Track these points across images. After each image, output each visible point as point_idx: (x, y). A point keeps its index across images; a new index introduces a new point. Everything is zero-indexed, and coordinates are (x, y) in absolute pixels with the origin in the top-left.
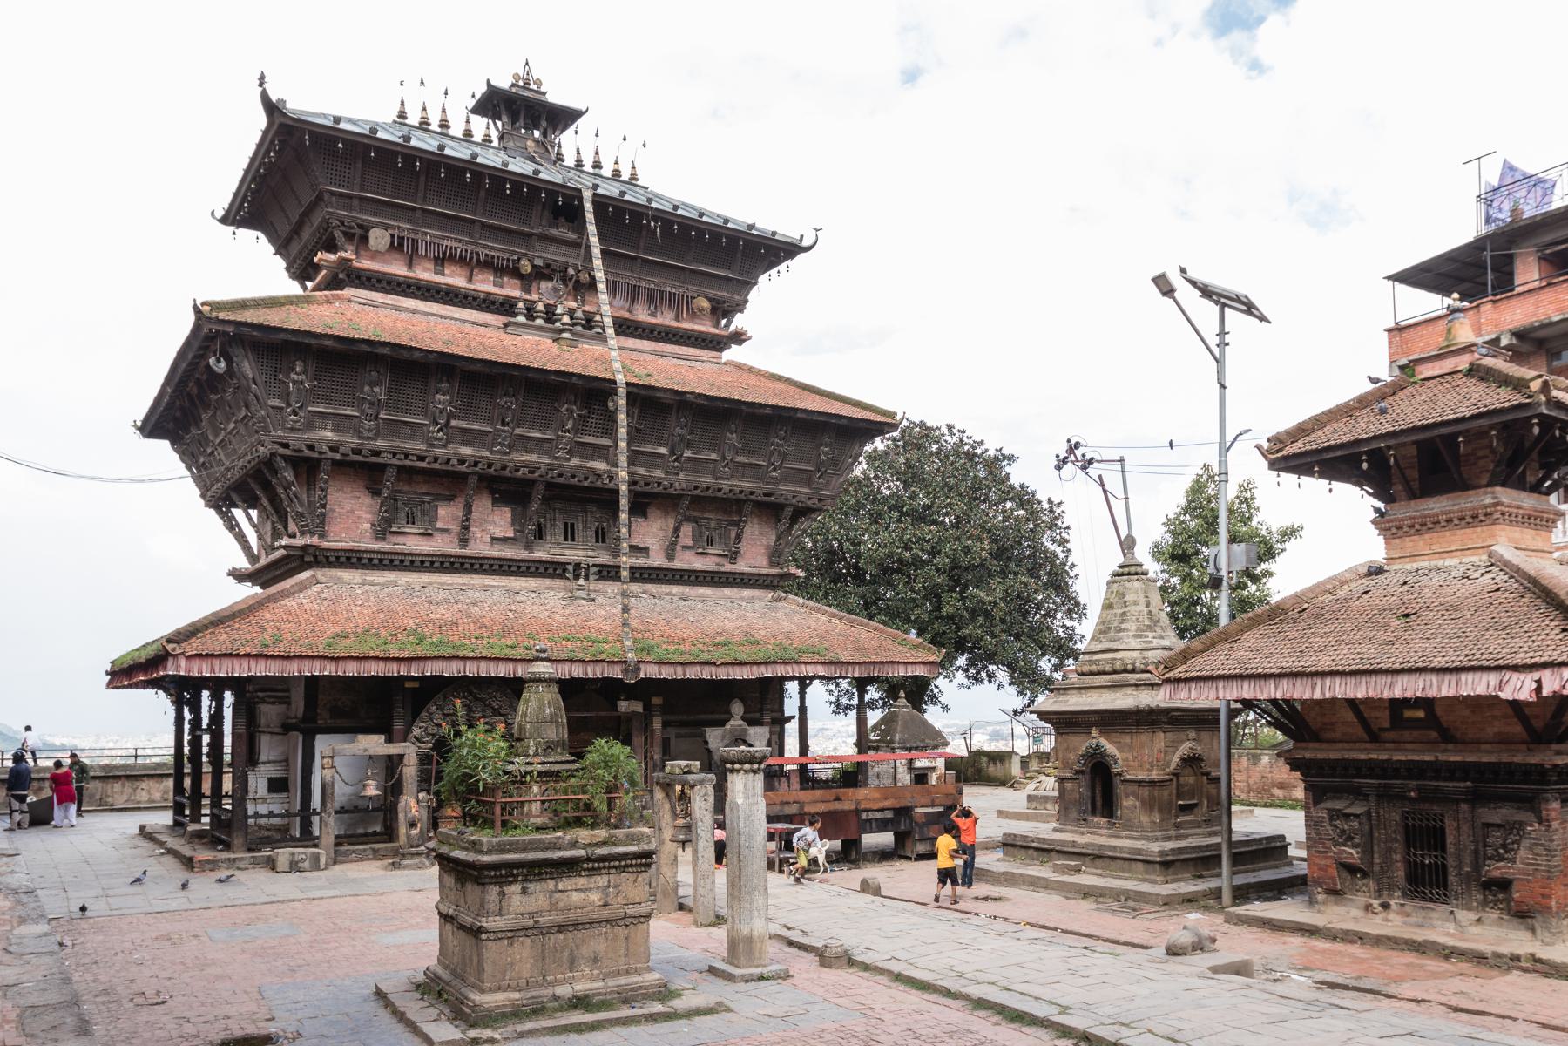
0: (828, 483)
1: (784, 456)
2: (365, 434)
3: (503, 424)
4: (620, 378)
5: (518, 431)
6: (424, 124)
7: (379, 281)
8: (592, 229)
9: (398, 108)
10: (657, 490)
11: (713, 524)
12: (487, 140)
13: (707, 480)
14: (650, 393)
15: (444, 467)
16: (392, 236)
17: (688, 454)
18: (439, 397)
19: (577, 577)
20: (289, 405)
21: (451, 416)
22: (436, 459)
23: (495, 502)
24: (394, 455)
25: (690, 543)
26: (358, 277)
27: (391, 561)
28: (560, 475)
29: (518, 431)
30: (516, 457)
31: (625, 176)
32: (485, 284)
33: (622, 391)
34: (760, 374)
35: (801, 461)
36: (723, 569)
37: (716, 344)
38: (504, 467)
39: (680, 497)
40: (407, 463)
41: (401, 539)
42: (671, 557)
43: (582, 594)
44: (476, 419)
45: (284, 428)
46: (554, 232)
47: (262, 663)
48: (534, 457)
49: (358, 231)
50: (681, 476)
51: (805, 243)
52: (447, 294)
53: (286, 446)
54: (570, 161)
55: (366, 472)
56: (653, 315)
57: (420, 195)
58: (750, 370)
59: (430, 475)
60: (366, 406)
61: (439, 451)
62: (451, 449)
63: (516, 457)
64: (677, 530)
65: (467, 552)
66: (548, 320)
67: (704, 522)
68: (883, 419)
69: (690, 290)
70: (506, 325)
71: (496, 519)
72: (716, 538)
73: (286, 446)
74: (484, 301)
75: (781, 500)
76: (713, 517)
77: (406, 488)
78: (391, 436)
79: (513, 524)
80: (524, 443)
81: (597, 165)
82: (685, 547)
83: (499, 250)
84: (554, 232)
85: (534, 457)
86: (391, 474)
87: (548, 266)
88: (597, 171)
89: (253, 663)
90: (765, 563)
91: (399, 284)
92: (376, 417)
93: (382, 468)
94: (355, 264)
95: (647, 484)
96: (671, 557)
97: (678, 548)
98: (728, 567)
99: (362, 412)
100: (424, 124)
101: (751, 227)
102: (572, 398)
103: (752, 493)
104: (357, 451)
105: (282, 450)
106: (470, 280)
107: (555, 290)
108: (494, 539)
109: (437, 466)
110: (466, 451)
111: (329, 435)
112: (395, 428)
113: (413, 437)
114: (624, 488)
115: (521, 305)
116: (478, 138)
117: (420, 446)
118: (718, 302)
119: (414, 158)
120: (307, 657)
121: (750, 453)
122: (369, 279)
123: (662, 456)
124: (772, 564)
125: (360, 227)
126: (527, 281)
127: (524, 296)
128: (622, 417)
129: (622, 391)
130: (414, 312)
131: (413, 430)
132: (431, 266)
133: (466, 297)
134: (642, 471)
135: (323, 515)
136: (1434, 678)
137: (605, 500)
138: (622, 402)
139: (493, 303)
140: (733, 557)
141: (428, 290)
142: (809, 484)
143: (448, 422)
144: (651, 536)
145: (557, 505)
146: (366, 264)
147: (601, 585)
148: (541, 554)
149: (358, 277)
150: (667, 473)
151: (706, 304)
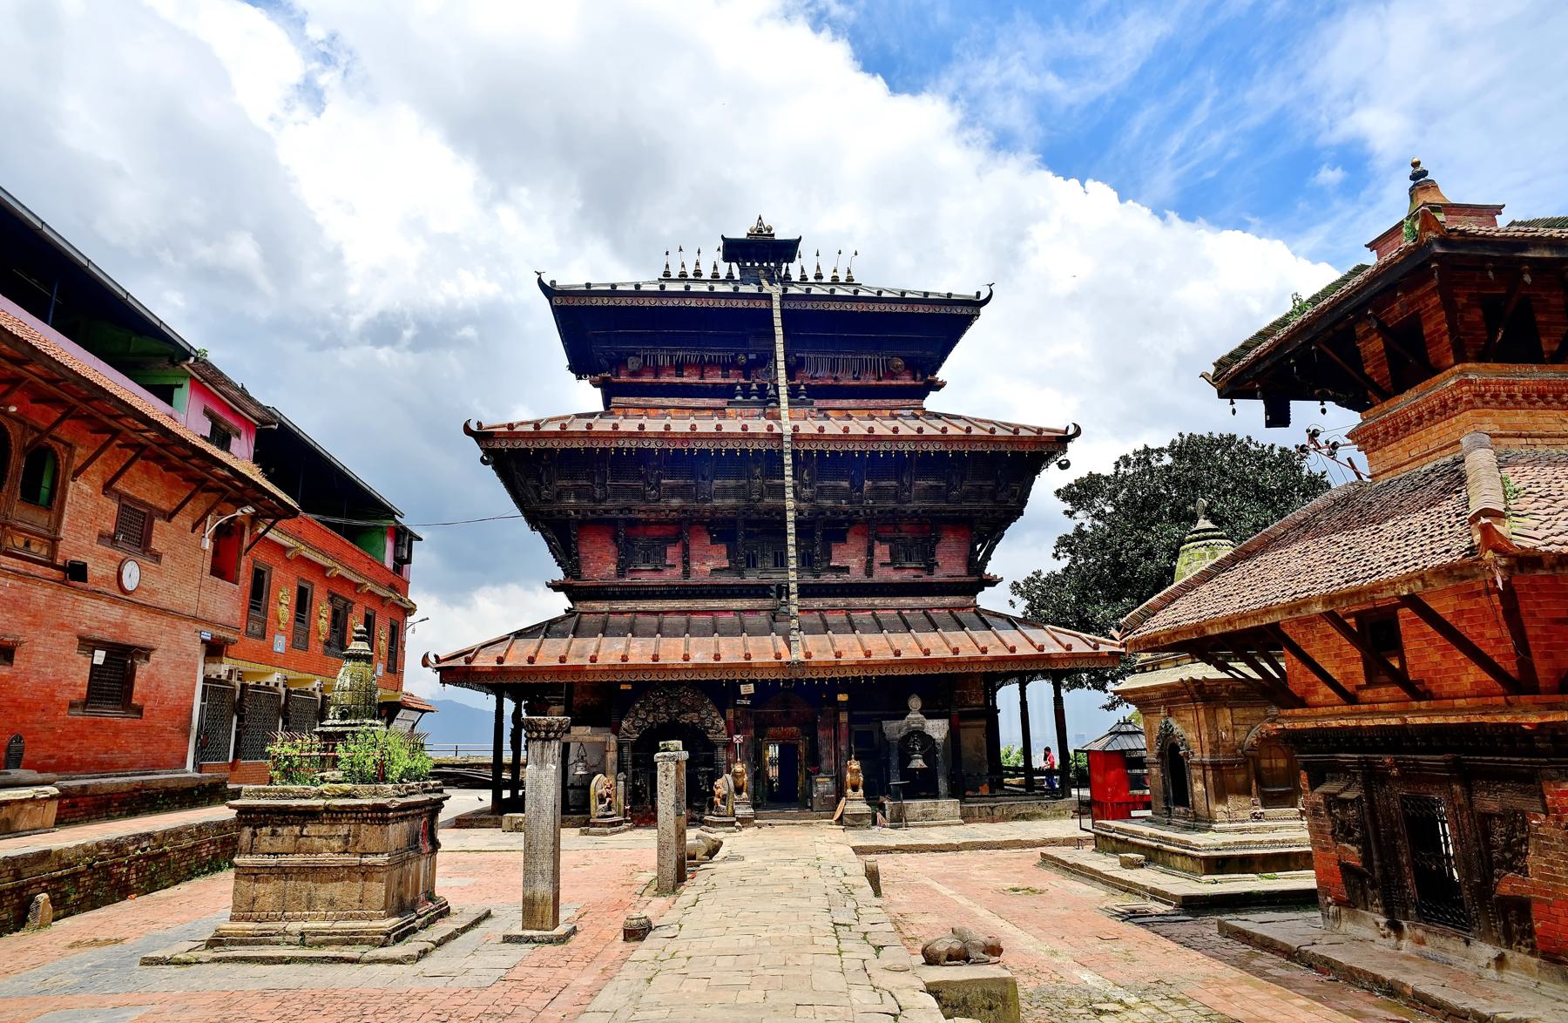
1: (963, 478)
6: (683, 276)
12: (730, 277)
13: (891, 504)
17: (868, 483)
19: (779, 597)
23: (713, 541)
31: (842, 279)
41: (638, 575)
51: (982, 297)
61: (653, 506)
63: (717, 502)
64: (870, 552)
65: (690, 581)
79: (730, 555)
80: (724, 493)
81: (819, 276)
90: (964, 572)
92: (603, 485)
93: (613, 523)
95: (834, 513)
96: (869, 572)
97: (876, 563)
98: (925, 578)
100: (683, 276)
101: (949, 295)
104: (593, 512)
106: (702, 377)
114: (790, 516)
116: (723, 276)
123: (845, 489)
124: (969, 574)
126: (747, 370)
127: (742, 380)
134: (829, 503)
140: (930, 569)
143: (658, 484)
148: (752, 578)
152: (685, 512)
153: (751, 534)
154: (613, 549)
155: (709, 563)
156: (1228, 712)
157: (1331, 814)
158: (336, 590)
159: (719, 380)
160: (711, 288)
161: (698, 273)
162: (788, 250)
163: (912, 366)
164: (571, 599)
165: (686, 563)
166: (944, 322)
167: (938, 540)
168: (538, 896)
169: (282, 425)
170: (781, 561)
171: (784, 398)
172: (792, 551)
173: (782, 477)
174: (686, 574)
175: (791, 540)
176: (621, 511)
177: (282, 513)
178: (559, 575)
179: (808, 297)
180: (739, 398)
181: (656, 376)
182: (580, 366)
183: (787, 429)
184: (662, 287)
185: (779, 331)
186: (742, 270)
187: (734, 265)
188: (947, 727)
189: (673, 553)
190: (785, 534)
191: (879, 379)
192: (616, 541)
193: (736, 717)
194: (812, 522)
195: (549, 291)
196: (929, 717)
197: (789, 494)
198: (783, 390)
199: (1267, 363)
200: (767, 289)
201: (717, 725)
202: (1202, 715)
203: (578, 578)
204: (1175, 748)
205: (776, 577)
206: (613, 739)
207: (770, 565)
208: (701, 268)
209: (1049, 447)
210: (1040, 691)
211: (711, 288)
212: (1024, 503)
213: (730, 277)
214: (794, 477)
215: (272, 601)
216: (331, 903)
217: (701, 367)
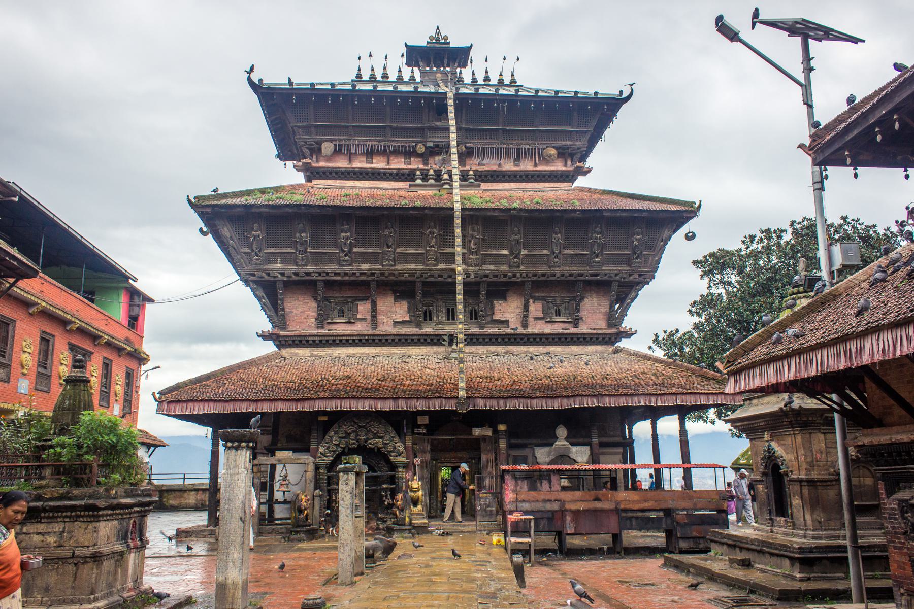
0: (646, 261)
1: (603, 246)
2: (300, 263)
3: (388, 247)
4: (458, 206)
5: (399, 250)
6: (373, 78)
7: (330, 173)
8: (452, 115)
9: (356, 72)
10: (503, 279)
11: (558, 301)
12: (412, 79)
13: (544, 269)
14: (483, 213)
15: (352, 278)
16: (335, 145)
17: (524, 252)
18: (343, 234)
19: (451, 344)
20: (253, 251)
21: (352, 246)
22: (346, 274)
23: (397, 299)
24: (320, 274)
25: (541, 315)
26: (318, 173)
27: (327, 341)
28: (432, 276)
29: (399, 250)
30: (399, 267)
31: (507, 81)
32: (399, 164)
33: (458, 214)
34: (595, 191)
35: (615, 248)
36: (566, 332)
37: (568, 177)
38: (393, 274)
39: (522, 284)
40: (328, 278)
41: (334, 327)
42: (525, 326)
43: (454, 355)
44: (370, 246)
45: (252, 265)
46: (439, 124)
47: (212, 404)
48: (413, 266)
49: (316, 146)
50: (522, 268)
51: (624, 96)
52: (373, 174)
53: (253, 275)
54: (467, 79)
55: (303, 285)
56: (515, 166)
57: (350, 117)
58: (589, 190)
59: (340, 285)
60: (299, 246)
62: (355, 267)
63: (399, 267)
64: (526, 308)
65: (376, 332)
66: (435, 180)
67: (550, 300)
68: (682, 208)
69: (540, 144)
70: (410, 186)
71: (398, 309)
72: (563, 311)
73: (253, 275)
74: (397, 174)
75: (606, 278)
76: (558, 295)
77: (337, 295)
78: (316, 262)
79: (409, 312)
80: (405, 258)
81: (487, 79)
82: (536, 319)
83: (402, 141)
84: (439, 124)
85: (413, 266)
86: (320, 285)
87: (437, 146)
88: (487, 83)
89: (206, 405)
91: (343, 173)
92: (305, 251)
94: (314, 165)
95: (496, 276)
97: (531, 318)
98: (572, 330)
99: (296, 249)
100: (373, 78)
101: (596, 93)
102: (432, 224)
103: (582, 275)
104: (296, 274)
105: (252, 278)
106: (388, 163)
107: (443, 159)
108: (396, 323)
109: (347, 278)
110: (365, 266)
111: (279, 265)
112: (318, 258)
113: (331, 262)
114: (459, 278)
115: (418, 173)
116: (406, 78)
117: (334, 266)
118: (563, 149)
119: (339, 96)
120: (238, 400)
121: (575, 246)
122: (324, 173)
124: (610, 326)
125: (317, 143)
126: (425, 157)
127: (421, 166)
128: (458, 231)
129: (458, 214)
130: (352, 188)
131: (330, 258)
132: (364, 159)
133: (385, 174)
134: (492, 267)
135: (283, 315)
136: (887, 336)
137: (445, 288)
138: (458, 221)
139: (403, 175)
140: (576, 325)
141: (361, 174)
142: (629, 264)
143: (350, 251)
144: (508, 311)
145: (439, 297)
146: (322, 164)
147: (473, 349)
148: (428, 330)
149: (318, 173)
150: (510, 267)
151: (553, 152)
152: (373, 274)
153: (427, 295)
154: (314, 305)
155: (393, 313)
156: (822, 436)
157: (904, 518)
158: (74, 341)
159: (402, 166)
160: (395, 88)
161: (385, 76)
162: (461, 56)
163: (563, 154)
164: (277, 346)
165: (374, 317)
166: (591, 115)
167: (583, 299)
168: (230, 581)
169: (22, 198)
170: (451, 315)
171: (456, 178)
172: (460, 307)
173: (453, 246)
174: (374, 325)
175: (460, 297)
176: (320, 274)
177: (24, 273)
178: (268, 327)
179: (476, 98)
180: (419, 181)
181: (350, 161)
182: (285, 153)
183: (458, 206)
184: (354, 86)
185: (452, 122)
186: (423, 74)
187: (416, 69)
188: (588, 452)
189: (363, 308)
190: (454, 293)
191: (536, 165)
192: (315, 298)
193: (414, 443)
194: (478, 284)
195: (256, 87)
196: (573, 444)
197: (459, 259)
198: (456, 172)
199: (855, 132)
200: (443, 89)
201: (398, 448)
202: (799, 438)
203: (284, 329)
204: (776, 468)
205: (448, 329)
206: (311, 459)
207: (444, 319)
208: (388, 71)
209: (674, 217)
210: (669, 425)
211: (395, 88)
212: (655, 269)
213: (412, 79)
214: (463, 246)
215: (16, 349)
216: (47, 589)
217: (387, 153)
